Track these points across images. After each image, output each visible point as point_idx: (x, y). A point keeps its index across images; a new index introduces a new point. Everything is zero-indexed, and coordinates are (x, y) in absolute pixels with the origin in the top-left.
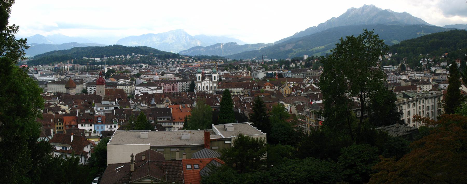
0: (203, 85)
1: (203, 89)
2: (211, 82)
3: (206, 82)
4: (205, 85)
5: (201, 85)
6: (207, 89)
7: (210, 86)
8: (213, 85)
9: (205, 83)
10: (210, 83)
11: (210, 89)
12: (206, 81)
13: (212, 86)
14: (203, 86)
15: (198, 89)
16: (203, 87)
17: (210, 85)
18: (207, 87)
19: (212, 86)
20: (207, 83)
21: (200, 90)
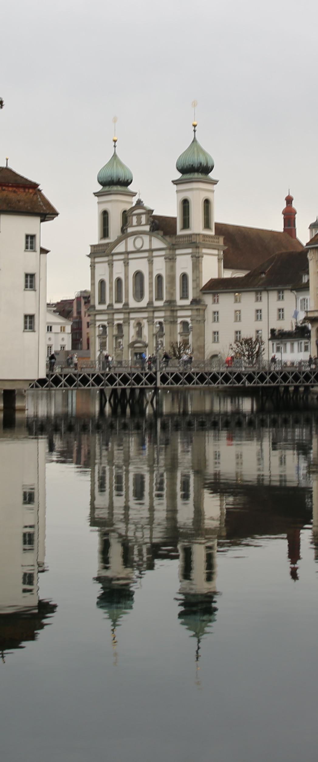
0: (119, 270)
1: (119, 300)
3: (131, 248)
6: (139, 294)
7: (151, 273)
8: (172, 269)
9: (128, 253)
10: (151, 251)
11: (151, 292)
12: (130, 240)
14: (115, 277)
16: (119, 280)
17: (151, 262)
18: (139, 275)
20: (139, 251)
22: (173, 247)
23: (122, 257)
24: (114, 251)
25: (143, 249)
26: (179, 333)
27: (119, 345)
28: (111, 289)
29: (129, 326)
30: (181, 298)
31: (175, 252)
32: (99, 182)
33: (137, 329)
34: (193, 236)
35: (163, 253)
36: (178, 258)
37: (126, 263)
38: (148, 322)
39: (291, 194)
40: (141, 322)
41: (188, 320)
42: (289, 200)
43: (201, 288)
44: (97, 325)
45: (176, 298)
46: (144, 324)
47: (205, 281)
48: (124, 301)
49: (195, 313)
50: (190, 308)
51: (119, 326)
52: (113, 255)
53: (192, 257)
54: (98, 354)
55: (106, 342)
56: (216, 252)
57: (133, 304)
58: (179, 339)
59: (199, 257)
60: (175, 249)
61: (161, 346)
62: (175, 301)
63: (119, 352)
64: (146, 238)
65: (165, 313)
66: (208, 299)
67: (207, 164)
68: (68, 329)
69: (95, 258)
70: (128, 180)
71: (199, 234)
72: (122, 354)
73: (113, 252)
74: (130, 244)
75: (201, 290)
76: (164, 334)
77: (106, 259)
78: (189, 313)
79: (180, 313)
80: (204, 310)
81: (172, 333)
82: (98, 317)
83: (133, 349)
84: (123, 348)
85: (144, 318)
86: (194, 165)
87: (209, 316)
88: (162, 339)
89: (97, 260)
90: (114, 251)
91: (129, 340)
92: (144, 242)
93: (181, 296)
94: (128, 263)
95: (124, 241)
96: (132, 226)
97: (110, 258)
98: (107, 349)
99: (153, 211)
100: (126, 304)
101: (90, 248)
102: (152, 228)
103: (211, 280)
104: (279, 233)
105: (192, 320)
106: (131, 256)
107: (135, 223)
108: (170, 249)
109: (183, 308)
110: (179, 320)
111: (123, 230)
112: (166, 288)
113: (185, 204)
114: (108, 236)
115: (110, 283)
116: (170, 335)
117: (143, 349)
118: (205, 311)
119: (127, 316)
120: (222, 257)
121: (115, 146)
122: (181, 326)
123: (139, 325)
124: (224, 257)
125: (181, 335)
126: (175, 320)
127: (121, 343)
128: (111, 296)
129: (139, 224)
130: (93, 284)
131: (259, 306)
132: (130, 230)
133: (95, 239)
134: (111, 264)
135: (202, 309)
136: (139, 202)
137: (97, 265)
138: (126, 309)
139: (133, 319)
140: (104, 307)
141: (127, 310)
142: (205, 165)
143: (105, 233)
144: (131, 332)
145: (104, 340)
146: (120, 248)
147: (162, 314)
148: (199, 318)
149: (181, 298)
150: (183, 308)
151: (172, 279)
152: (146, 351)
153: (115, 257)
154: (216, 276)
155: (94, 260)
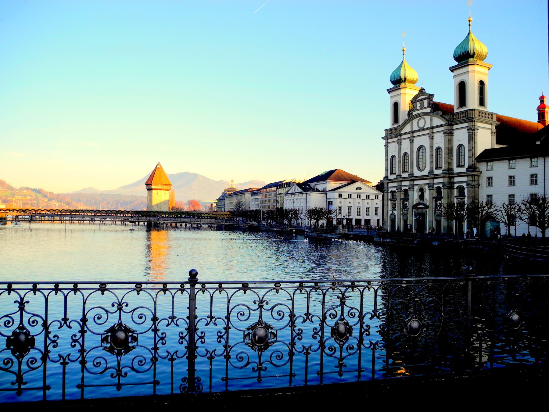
0: (406, 146)
1: (404, 172)
3: (415, 128)
4: (412, 141)
9: (413, 132)
10: (432, 128)
11: (431, 162)
12: (415, 122)
13: (442, 146)
16: (405, 154)
17: (432, 138)
19: (442, 146)
20: (422, 129)
22: (451, 123)
23: (408, 136)
24: (402, 132)
25: (425, 127)
26: (455, 197)
27: (405, 206)
28: (400, 162)
29: (413, 191)
30: (458, 166)
31: (453, 128)
32: (391, 81)
33: (420, 193)
34: (469, 112)
35: (442, 129)
36: (455, 132)
37: (411, 140)
38: (429, 187)
39: (544, 95)
40: (423, 187)
41: (464, 185)
42: (542, 99)
43: (476, 157)
44: (389, 191)
45: (453, 166)
46: (426, 189)
47: (479, 150)
48: (409, 172)
49: (471, 178)
50: (466, 174)
51: (406, 191)
52: (401, 135)
53: (468, 130)
54: (390, 213)
55: (396, 204)
56: (489, 126)
57: (417, 173)
58: (455, 201)
59: (474, 130)
60: (453, 125)
61: (440, 208)
62: (452, 169)
63: (406, 212)
64: (428, 118)
65: (443, 180)
66: (482, 166)
67: (482, 50)
68: (380, 197)
69: (388, 139)
70: (414, 78)
71: (475, 110)
72: (408, 214)
73: (401, 133)
74: (415, 125)
75: (476, 159)
76: (443, 198)
77: (396, 139)
78: (465, 179)
79: (456, 179)
80: (479, 176)
81: (450, 196)
82: (390, 185)
83: (416, 210)
84: (408, 209)
85: (425, 184)
86: (469, 52)
87: (483, 181)
88: (440, 202)
89: (389, 141)
90: (402, 132)
91: (413, 203)
92: (426, 122)
93: (458, 165)
94: (413, 140)
95: (410, 123)
96: (416, 110)
97: (399, 137)
98: (397, 210)
99: (433, 95)
101: (384, 132)
102: (432, 110)
103: (486, 150)
104: (536, 123)
105: (467, 185)
106: (415, 134)
107: (418, 108)
108: (448, 125)
109: (459, 175)
110: (456, 186)
111: (409, 113)
112: (444, 158)
113: (462, 87)
114: (398, 122)
115: (398, 158)
116: (448, 198)
117: (425, 210)
118: (480, 177)
119: (411, 183)
120: (494, 130)
122: (458, 190)
123: (422, 190)
124: (496, 131)
125: (457, 199)
126: (452, 185)
127: (407, 205)
128: (400, 168)
129: (422, 107)
130: (387, 160)
131: (533, 171)
132: (414, 113)
133: (388, 124)
134: (399, 143)
135: (477, 176)
136: (422, 91)
137: (389, 145)
138: (411, 177)
139: (417, 185)
140: (394, 177)
141: (412, 178)
142: (480, 51)
143: (396, 119)
144: (415, 196)
145: (394, 203)
146: (407, 129)
147: (441, 180)
148: (473, 183)
149: (458, 166)
150: (459, 175)
151: (450, 151)
152: (427, 211)
153: (403, 137)
154: (489, 147)
155: (387, 141)
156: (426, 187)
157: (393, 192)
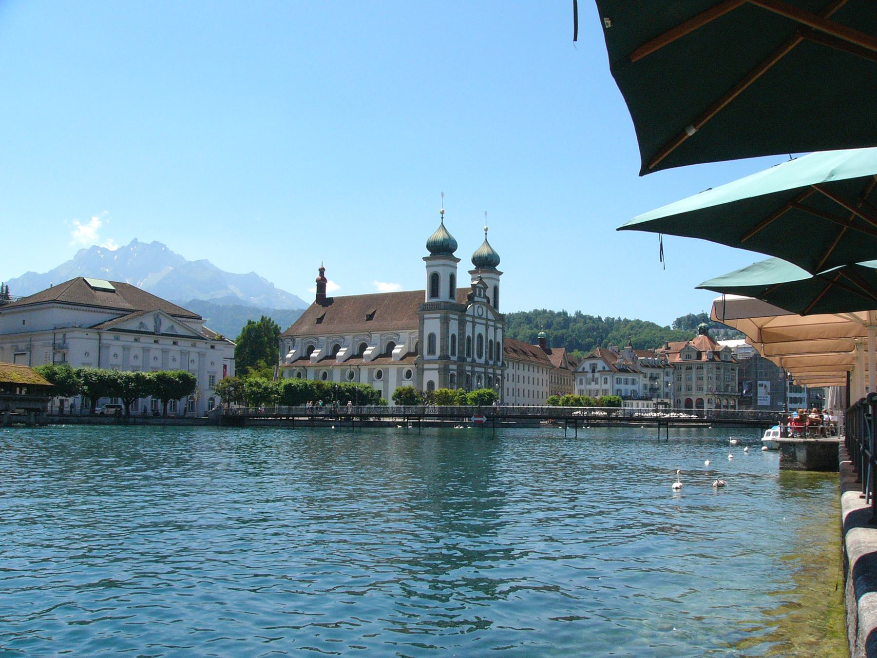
1: (469, 355)
2: (490, 316)
3: (476, 315)
5: (462, 324)
7: (487, 338)
9: (473, 317)
10: (487, 319)
11: (486, 352)
15: (450, 354)
16: (469, 337)
17: (487, 330)
20: (480, 317)
21: (453, 354)
42: (322, 271)
57: (478, 360)
64: (485, 309)
85: (482, 372)
100: (474, 360)
121: (442, 218)
123: (479, 378)
139: (477, 372)
156: (483, 375)
157: (452, 376)
